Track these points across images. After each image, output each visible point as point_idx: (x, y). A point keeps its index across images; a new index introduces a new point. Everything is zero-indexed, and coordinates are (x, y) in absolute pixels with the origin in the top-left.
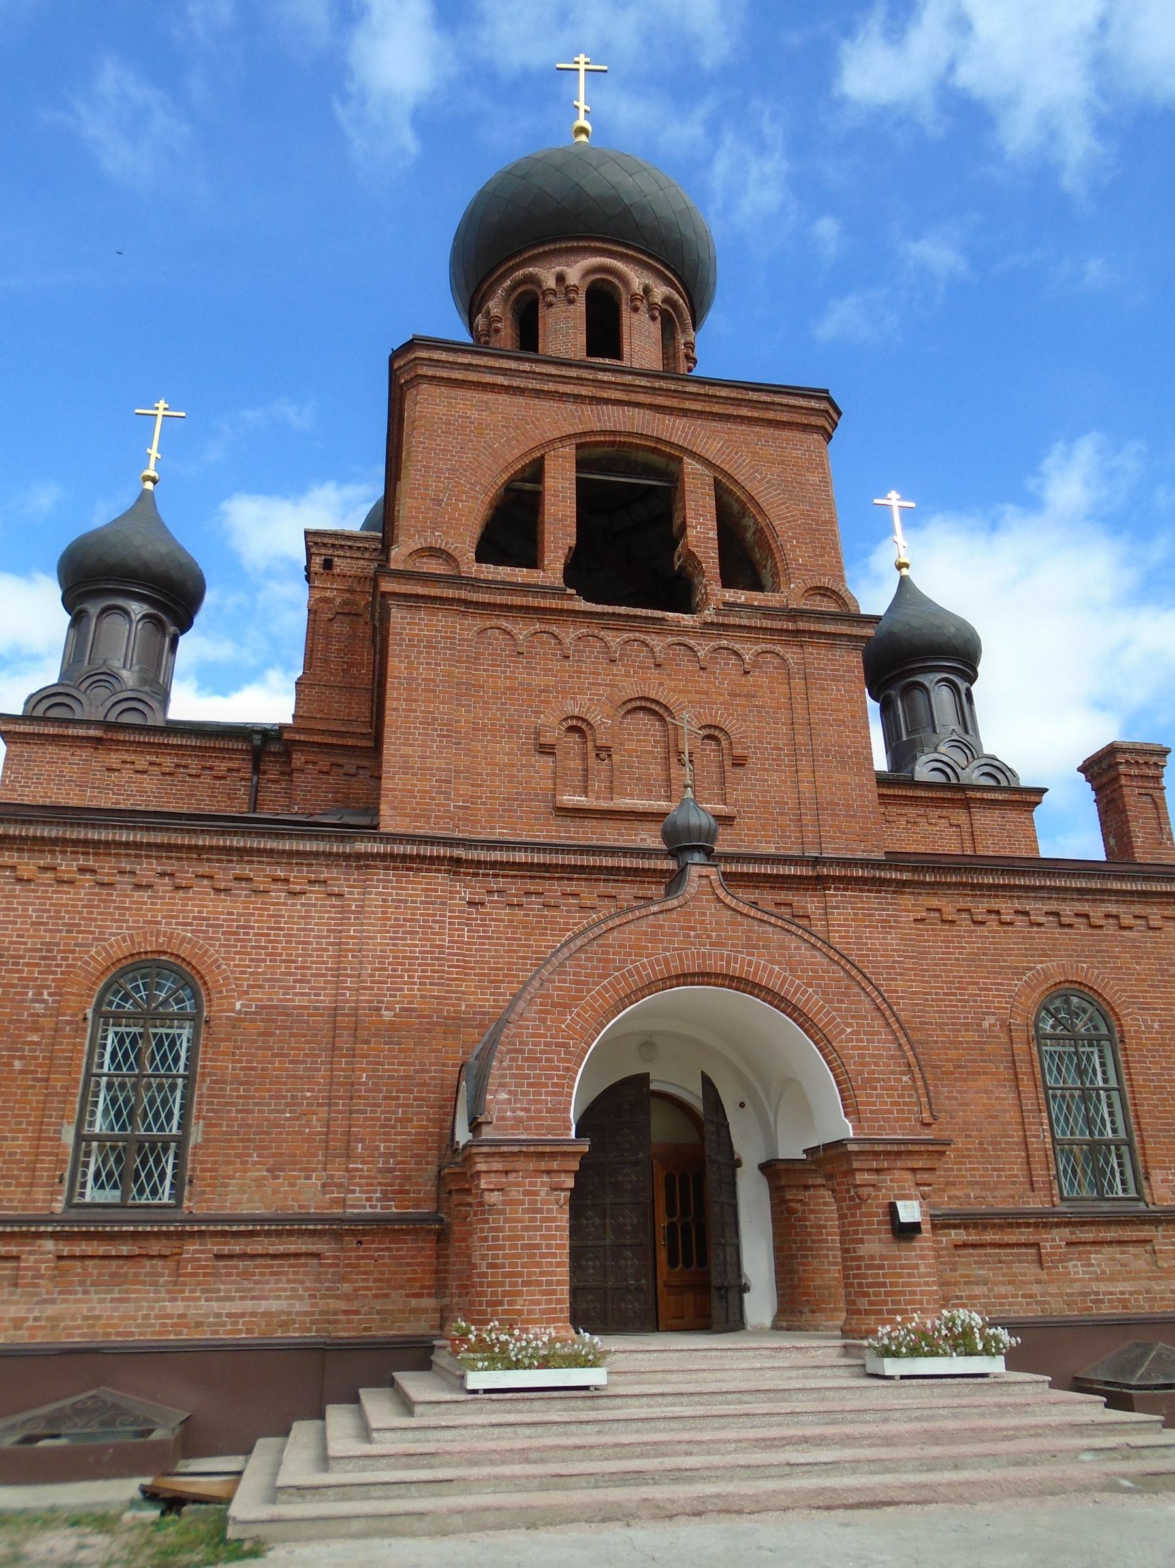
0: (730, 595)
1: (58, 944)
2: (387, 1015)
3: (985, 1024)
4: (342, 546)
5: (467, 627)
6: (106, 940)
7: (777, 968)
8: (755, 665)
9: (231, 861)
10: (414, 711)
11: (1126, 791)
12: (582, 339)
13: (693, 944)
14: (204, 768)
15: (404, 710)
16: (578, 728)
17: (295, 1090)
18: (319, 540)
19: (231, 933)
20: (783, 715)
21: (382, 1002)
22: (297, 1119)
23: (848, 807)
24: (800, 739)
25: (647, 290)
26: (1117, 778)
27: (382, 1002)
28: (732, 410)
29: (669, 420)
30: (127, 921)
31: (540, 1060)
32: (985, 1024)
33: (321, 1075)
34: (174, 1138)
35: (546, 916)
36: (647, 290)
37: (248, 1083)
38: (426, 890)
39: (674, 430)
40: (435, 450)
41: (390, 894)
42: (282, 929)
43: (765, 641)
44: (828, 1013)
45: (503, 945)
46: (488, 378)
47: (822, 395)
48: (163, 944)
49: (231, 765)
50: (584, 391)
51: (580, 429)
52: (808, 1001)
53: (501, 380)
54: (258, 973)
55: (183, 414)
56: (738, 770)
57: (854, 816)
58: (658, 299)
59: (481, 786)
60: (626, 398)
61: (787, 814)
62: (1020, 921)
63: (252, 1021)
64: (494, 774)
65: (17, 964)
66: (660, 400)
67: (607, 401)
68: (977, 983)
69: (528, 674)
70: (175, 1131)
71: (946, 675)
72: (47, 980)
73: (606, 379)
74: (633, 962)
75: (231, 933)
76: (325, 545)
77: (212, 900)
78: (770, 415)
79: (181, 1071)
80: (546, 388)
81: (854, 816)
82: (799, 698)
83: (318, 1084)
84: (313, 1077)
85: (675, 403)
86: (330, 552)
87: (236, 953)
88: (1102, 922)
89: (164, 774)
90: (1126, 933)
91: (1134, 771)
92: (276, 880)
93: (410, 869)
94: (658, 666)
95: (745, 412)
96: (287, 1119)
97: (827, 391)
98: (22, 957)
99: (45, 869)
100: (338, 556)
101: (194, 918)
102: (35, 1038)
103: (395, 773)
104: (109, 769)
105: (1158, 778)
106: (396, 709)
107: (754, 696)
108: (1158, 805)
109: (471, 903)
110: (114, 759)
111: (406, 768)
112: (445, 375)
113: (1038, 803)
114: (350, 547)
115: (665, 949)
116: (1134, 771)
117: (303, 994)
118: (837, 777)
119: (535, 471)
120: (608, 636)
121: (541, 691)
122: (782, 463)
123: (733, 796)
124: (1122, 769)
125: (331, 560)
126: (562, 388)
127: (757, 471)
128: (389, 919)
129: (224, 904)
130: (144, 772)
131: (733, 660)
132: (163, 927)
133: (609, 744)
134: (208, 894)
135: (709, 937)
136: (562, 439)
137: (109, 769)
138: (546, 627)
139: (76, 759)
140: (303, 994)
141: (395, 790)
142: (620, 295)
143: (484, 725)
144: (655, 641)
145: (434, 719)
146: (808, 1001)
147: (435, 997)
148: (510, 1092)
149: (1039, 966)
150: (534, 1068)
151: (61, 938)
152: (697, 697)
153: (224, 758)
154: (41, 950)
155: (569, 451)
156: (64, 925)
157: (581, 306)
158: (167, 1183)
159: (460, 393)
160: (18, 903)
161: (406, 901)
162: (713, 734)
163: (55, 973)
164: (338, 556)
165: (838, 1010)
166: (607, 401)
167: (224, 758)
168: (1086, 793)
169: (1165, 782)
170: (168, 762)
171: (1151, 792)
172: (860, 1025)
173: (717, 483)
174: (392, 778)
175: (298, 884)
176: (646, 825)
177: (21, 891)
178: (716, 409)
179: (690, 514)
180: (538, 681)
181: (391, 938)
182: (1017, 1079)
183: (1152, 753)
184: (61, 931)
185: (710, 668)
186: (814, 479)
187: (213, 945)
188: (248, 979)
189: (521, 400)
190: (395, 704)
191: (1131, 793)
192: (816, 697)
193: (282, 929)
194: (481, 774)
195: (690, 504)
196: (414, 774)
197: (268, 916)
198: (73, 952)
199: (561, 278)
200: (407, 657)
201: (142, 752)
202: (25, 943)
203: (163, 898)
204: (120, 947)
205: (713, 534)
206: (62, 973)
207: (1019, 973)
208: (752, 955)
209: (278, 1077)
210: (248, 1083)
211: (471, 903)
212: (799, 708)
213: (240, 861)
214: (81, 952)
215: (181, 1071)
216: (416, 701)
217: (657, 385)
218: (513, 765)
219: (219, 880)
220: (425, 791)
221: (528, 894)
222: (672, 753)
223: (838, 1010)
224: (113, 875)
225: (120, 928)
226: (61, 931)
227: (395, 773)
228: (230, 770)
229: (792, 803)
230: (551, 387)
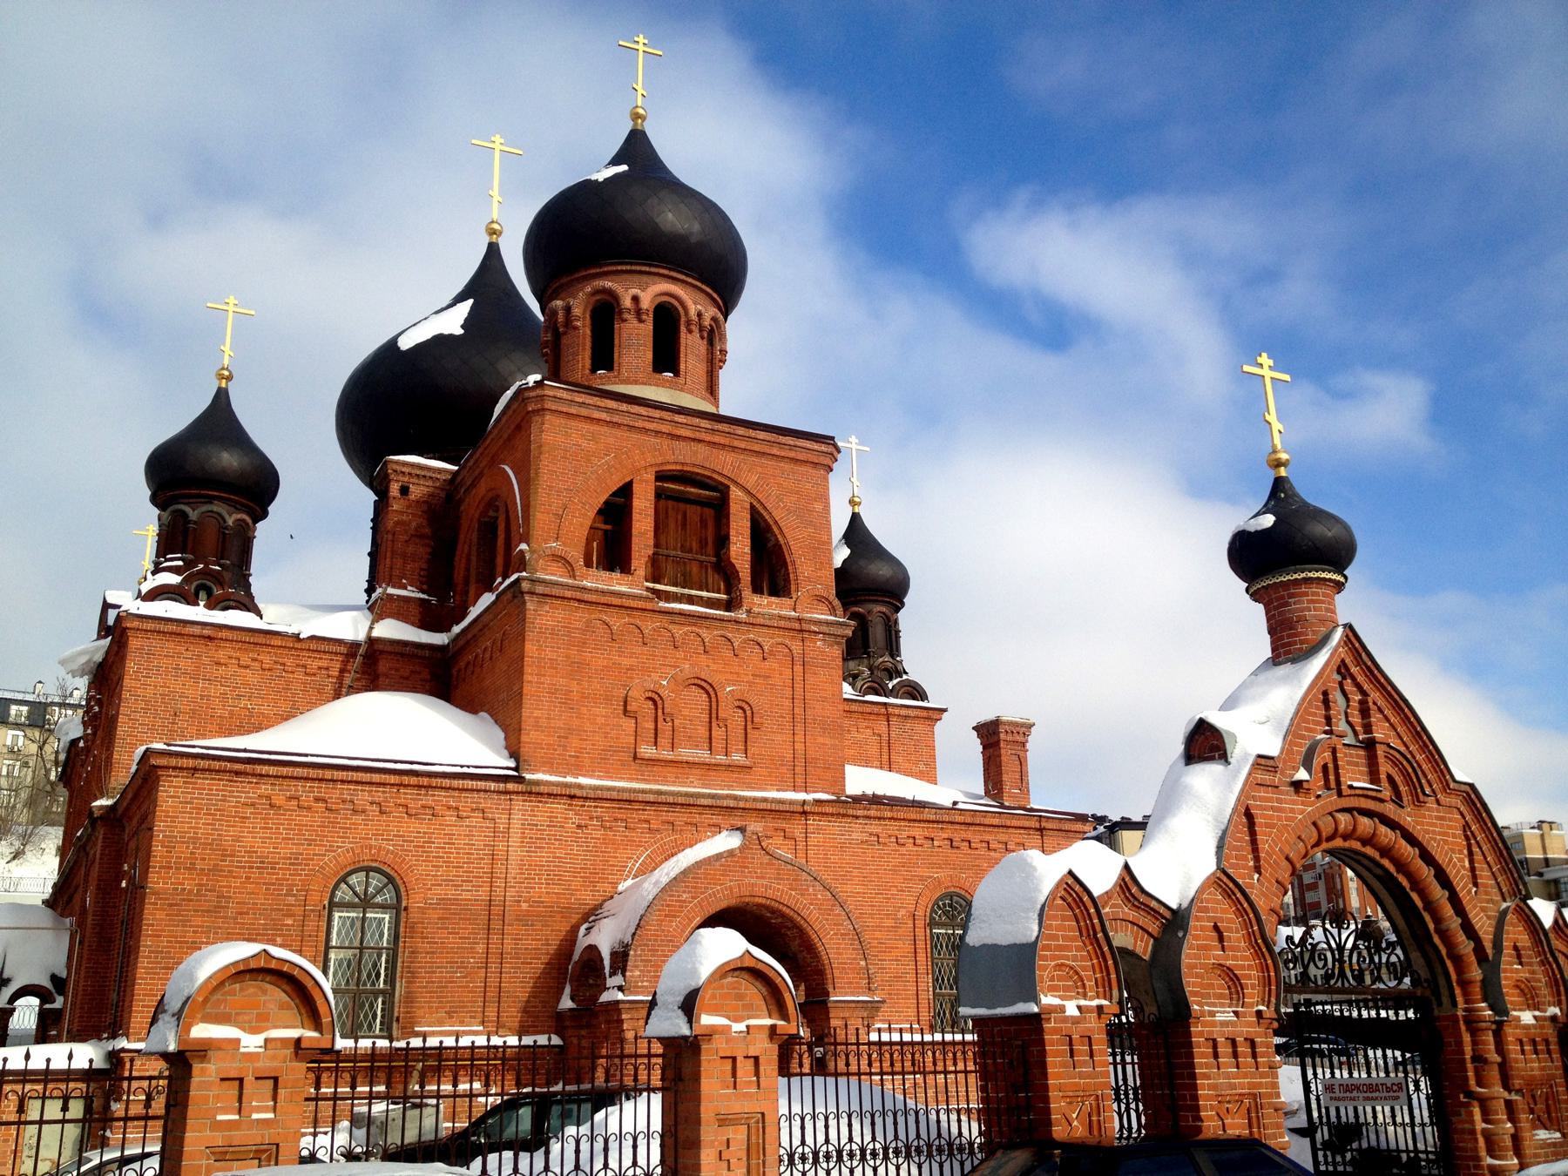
1: (302, 854)
2: (524, 906)
4: (418, 476)
5: (580, 617)
6: (334, 851)
7: (793, 893)
8: (771, 653)
9: (420, 795)
10: (543, 683)
11: (1003, 751)
12: (650, 355)
13: (746, 877)
14: (298, 666)
15: (537, 683)
16: (655, 700)
17: (463, 957)
19: (418, 847)
20: (788, 692)
21: (521, 896)
22: (464, 977)
24: (797, 710)
25: (699, 315)
26: (999, 741)
27: (521, 896)
28: (766, 449)
30: (349, 838)
31: (657, 951)
33: (480, 948)
34: (383, 992)
35: (627, 836)
36: (699, 315)
37: (433, 953)
38: (551, 817)
39: (721, 463)
40: (556, 472)
41: (527, 820)
42: (454, 844)
43: (779, 636)
44: (821, 922)
45: (599, 856)
46: (596, 415)
47: (827, 440)
48: (374, 855)
49: (324, 664)
51: (660, 460)
52: (810, 914)
53: (604, 416)
54: (437, 876)
55: (253, 313)
56: (756, 732)
57: (829, 768)
58: (707, 322)
59: (586, 740)
60: (692, 436)
61: (786, 765)
62: (928, 844)
63: (434, 909)
64: (595, 732)
65: (275, 868)
66: (717, 439)
67: (678, 437)
68: (896, 887)
69: (619, 656)
70: (382, 986)
72: (295, 880)
73: (680, 420)
74: (712, 889)
75: (418, 847)
76: (403, 473)
77: (406, 822)
78: (792, 454)
79: (385, 945)
80: (636, 424)
81: (829, 768)
82: (799, 678)
83: (478, 953)
84: (474, 948)
86: (406, 479)
87: (423, 861)
88: (979, 845)
89: (263, 670)
90: (992, 854)
92: (449, 808)
93: (540, 802)
95: (775, 451)
96: (457, 977)
97: (832, 438)
98: (278, 863)
99: (291, 798)
100: (413, 484)
101: (394, 836)
102: (290, 922)
103: (530, 730)
104: (218, 664)
105: (1024, 744)
106: (531, 682)
107: (769, 677)
108: (1022, 762)
109: (579, 827)
110: (221, 655)
111: (537, 727)
112: (564, 410)
113: (940, 719)
114: (424, 476)
115: (731, 881)
116: (1009, 738)
117: (468, 891)
118: (821, 740)
119: (626, 491)
120: (674, 628)
121: (628, 669)
122: (797, 493)
123: (751, 751)
124: (1002, 736)
125: (408, 488)
127: (781, 500)
128: (526, 838)
129: (414, 825)
130: (247, 667)
131: (757, 649)
132: (373, 843)
133: (673, 711)
134: (403, 818)
135: (756, 873)
136: (646, 468)
137: (218, 664)
138: (632, 621)
140: (468, 891)
141: (530, 743)
142: (680, 316)
143: (589, 694)
144: (704, 633)
145: (556, 690)
146: (810, 914)
147: (556, 893)
148: (640, 971)
149: (936, 875)
150: (654, 956)
151: (304, 849)
153: (316, 658)
154: (290, 858)
156: (306, 840)
157: (648, 327)
158: (378, 1021)
159: (573, 423)
160: (273, 824)
161: (537, 825)
162: (743, 706)
163: (301, 875)
164: (413, 484)
165: (827, 920)
166: (678, 437)
167: (316, 658)
168: (975, 746)
169: (1028, 746)
170: (267, 660)
171: (1019, 753)
172: (838, 930)
173: (752, 506)
174: (528, 734)
175: (464, 811)
176: (694, 771)
177: (274, 814)
178: (756, 448)
179: (732, 532)
180: (626, 662)
181: (527, 851)
182: (915, 952)
183: (1022, 725)
184: (303, 844)
185: (742, 655)
186: (818, 506)
187: (408, 856)
188: (431, 880)
189: (618, 433)
190: (530, 678)
191: (1006, 752)
192: (810, 679)
193: (454, 844)
194: (586, 731)
195: (733, 525)
196: (543, 731)
197: (445, 834)
198: (313, 860)
199: (635, 299)
200: (538, 641)
201: (246, 650)
202: (280, 853)
203: (373, 820)
204: (345, 857)
205: (747, 550)
206: (306, 875)
208: (778, 884)
209: (452, 948)
210: (433, 953)
211: (579, 827)
212: (799, 686)
213: (426, 795)
214: (319, 860)
215: (385, 945)
216: (545, 675)
217: (716, 427)
218: (608, 725)
219: (411, 808)
220: (550, 745)
221: (616, 820)
222: (713, 716)
223: (827, 920)
224: (338, 803)
225: (344, 842)
226: (303, 844)
227: (530, 730)
228: (320, 668)
229: (789, 756)
230: (640, 424)
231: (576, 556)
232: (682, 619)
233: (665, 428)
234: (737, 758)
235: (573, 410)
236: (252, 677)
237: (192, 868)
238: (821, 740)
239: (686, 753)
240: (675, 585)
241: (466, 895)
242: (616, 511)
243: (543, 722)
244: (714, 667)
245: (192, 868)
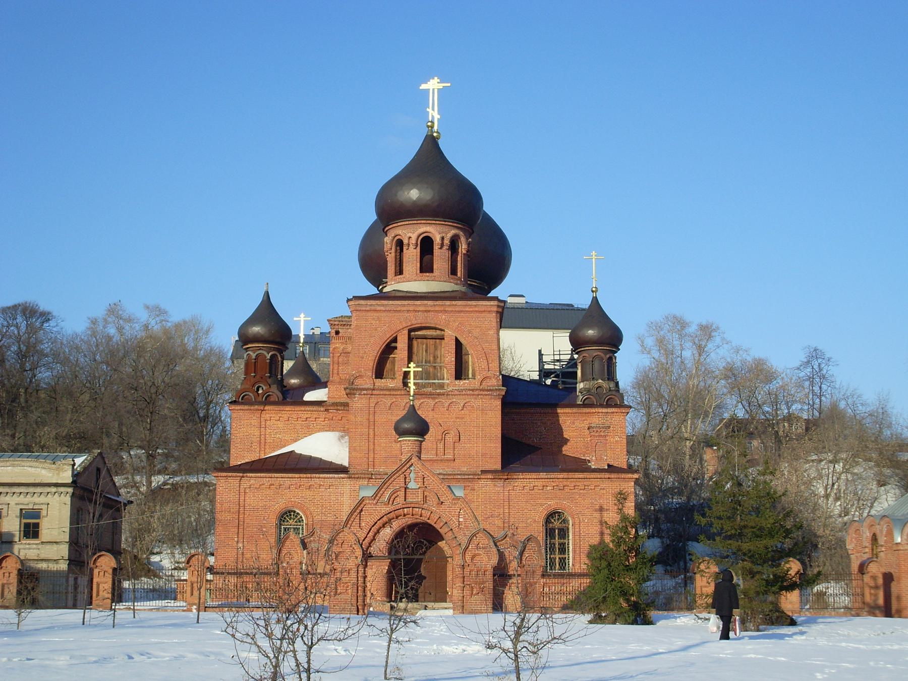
0: (457, 382)
3: (528, 521)
18: (331, 322)
32: (528, 521)
36: (443, 238)
51: (409, 324)
58: (447, 242)
66: (437, 309)
71: (599, 353)
78: (476, 309)
80: (398, 309)
91: (597, 434)
112: (364, 309)
119: (395, 340)
132: (293, 500)
136: (403, 328)
139: (255, 418)
155: (406, 332)
159: (369, 314)
205: (454, 359)
207: (542, 505)
231: (370, 373)
232: (420, 397)
233: (411, 308)
235: (368, 309)
236: (280, 425)
237: (229, 512)
240: (422, 379)
241: (329, 519)
242: (389, 348)
243: (358, 448)
245: (229, 512)
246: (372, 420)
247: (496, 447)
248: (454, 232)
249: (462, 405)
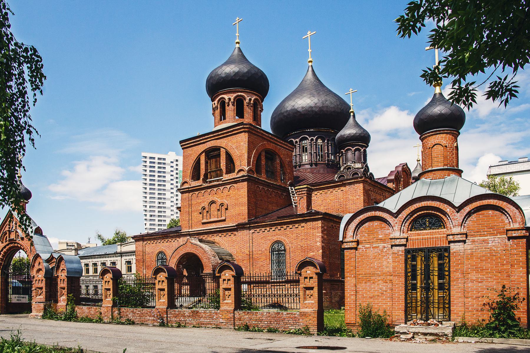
0: (226, 176)
23: (243, 214)
29: (219, 141)
46: (193, 144)
50: (204, 141)
53: (193, 144)
58: (232, 100)
78: (234, 132)
85: (218, 137)
94: (216, 194)
118: (241, 208)
126: (201, 142)
136: (202, 153)
152: (221, 198)
180: (200, 201)
205: (225, 163)
217: (214, 135)
234: (223, 218)
238: (241, 208)
239: (212, 220)
244: (217, 196)
246: (190, 203)
247: (245, 209)
248: (235, 95)
249: (228, 188)
